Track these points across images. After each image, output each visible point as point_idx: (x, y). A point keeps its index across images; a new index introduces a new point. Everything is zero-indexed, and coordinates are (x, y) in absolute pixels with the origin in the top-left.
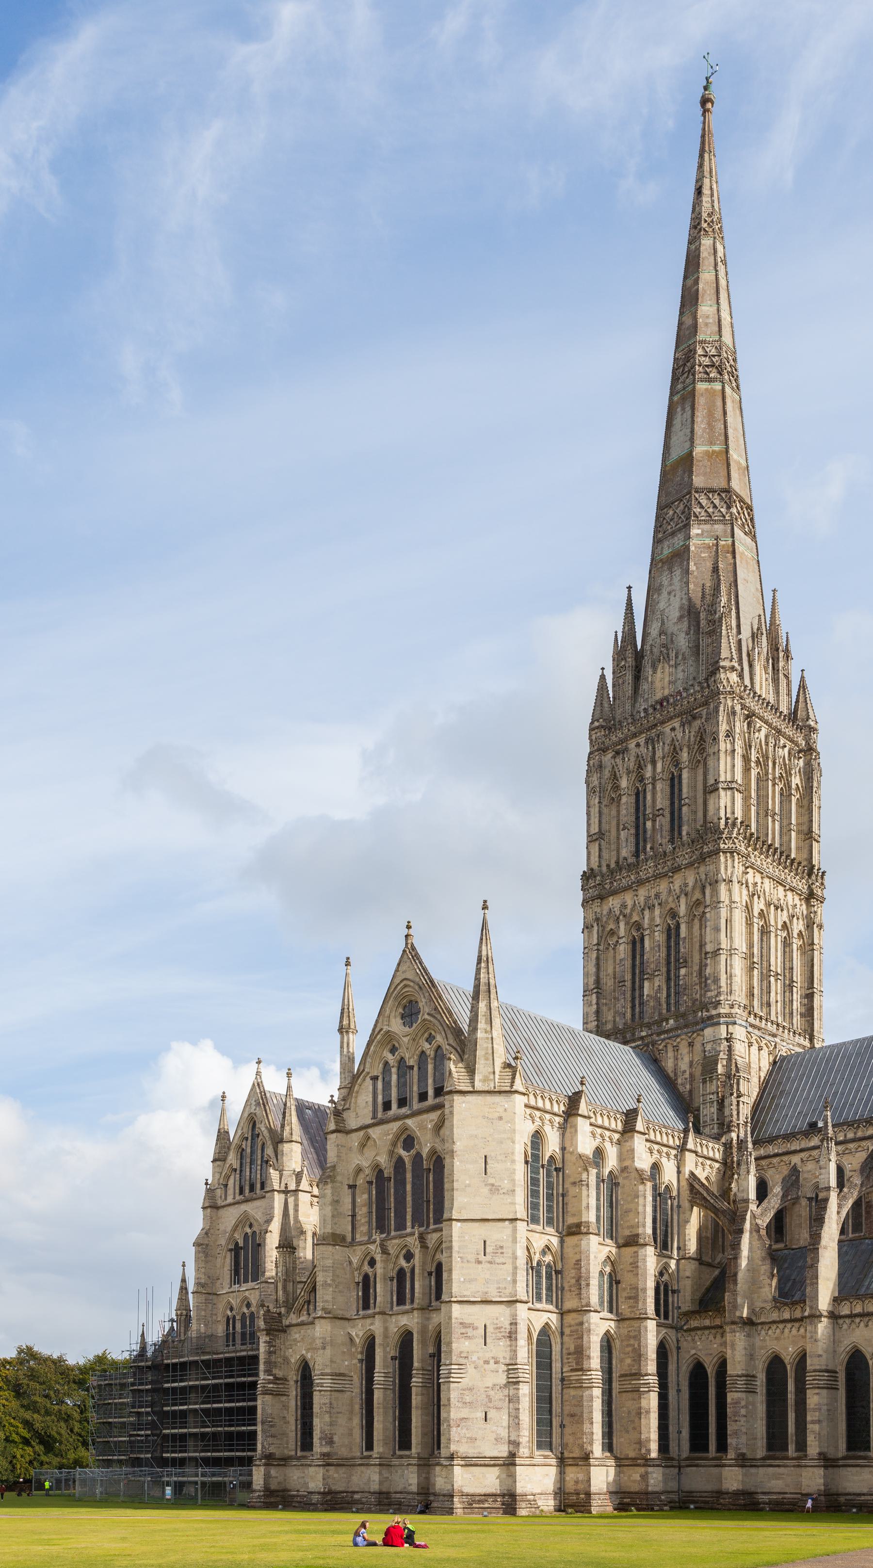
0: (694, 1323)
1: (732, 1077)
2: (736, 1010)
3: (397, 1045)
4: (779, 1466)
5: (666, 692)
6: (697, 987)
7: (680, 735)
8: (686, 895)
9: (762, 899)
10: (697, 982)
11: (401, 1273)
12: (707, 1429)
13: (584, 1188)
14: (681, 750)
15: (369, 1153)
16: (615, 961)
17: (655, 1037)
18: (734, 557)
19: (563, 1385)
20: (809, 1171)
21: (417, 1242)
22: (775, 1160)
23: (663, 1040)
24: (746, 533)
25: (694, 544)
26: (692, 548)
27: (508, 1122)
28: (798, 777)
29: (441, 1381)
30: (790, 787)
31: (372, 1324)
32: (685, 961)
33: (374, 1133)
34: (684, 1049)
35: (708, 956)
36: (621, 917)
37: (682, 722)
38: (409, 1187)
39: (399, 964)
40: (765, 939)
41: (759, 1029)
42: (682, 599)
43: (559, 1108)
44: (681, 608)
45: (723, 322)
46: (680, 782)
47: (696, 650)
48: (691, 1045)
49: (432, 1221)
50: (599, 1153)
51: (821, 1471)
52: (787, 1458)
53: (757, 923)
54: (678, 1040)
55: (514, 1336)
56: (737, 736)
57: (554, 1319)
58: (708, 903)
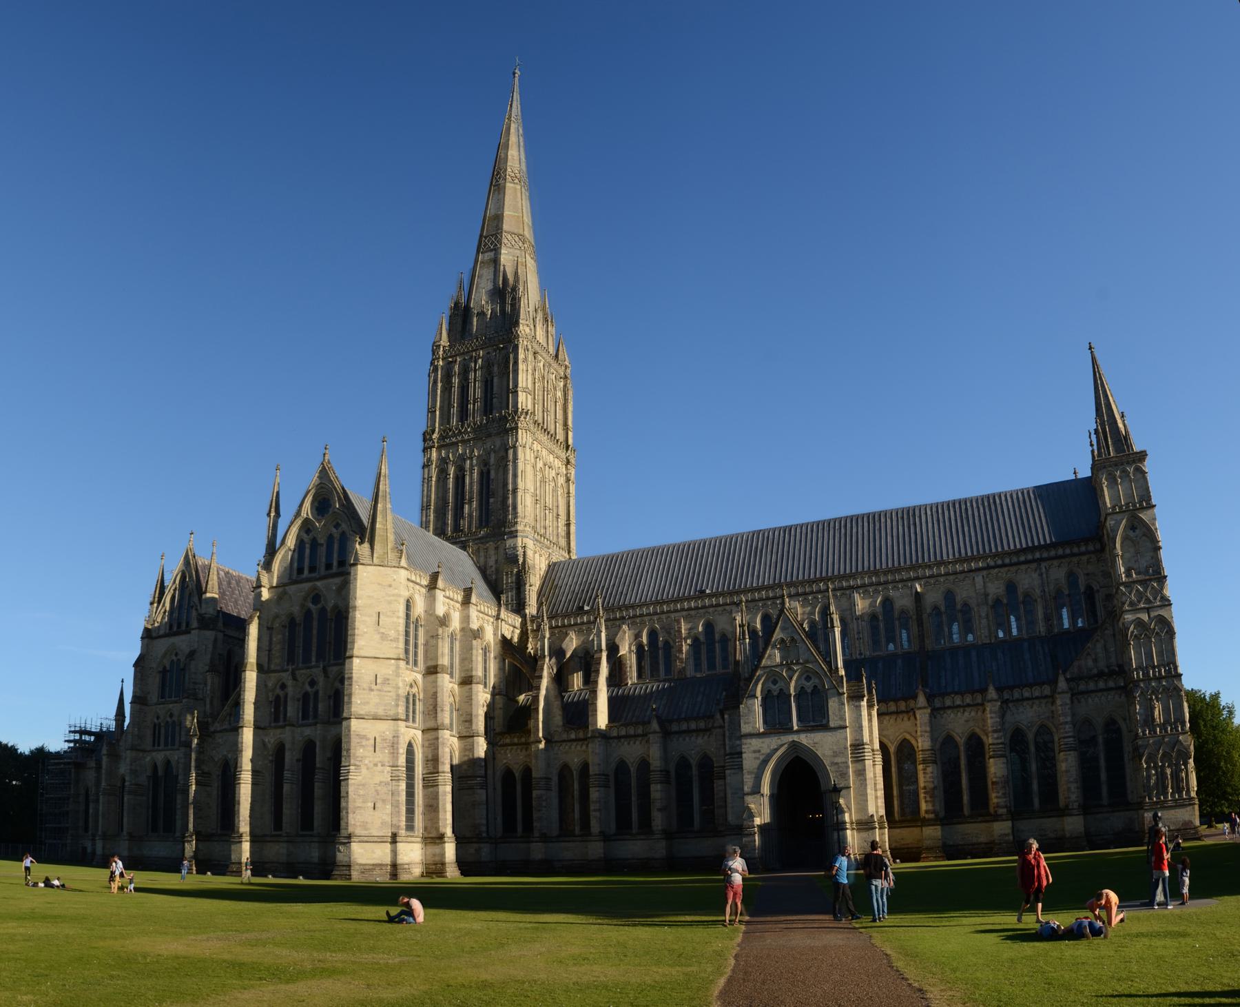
4: (569, 841)
8: (495, 452)
9: (541, 461)
13: (440, 640)
14: (493, 366)
31: (280, 734)
38: (315, 632)
43: (425, 582)
48: (497, 548)
49: (332, 658)
51: (602, 843)
52: (575, 836)
54: (487, 545)
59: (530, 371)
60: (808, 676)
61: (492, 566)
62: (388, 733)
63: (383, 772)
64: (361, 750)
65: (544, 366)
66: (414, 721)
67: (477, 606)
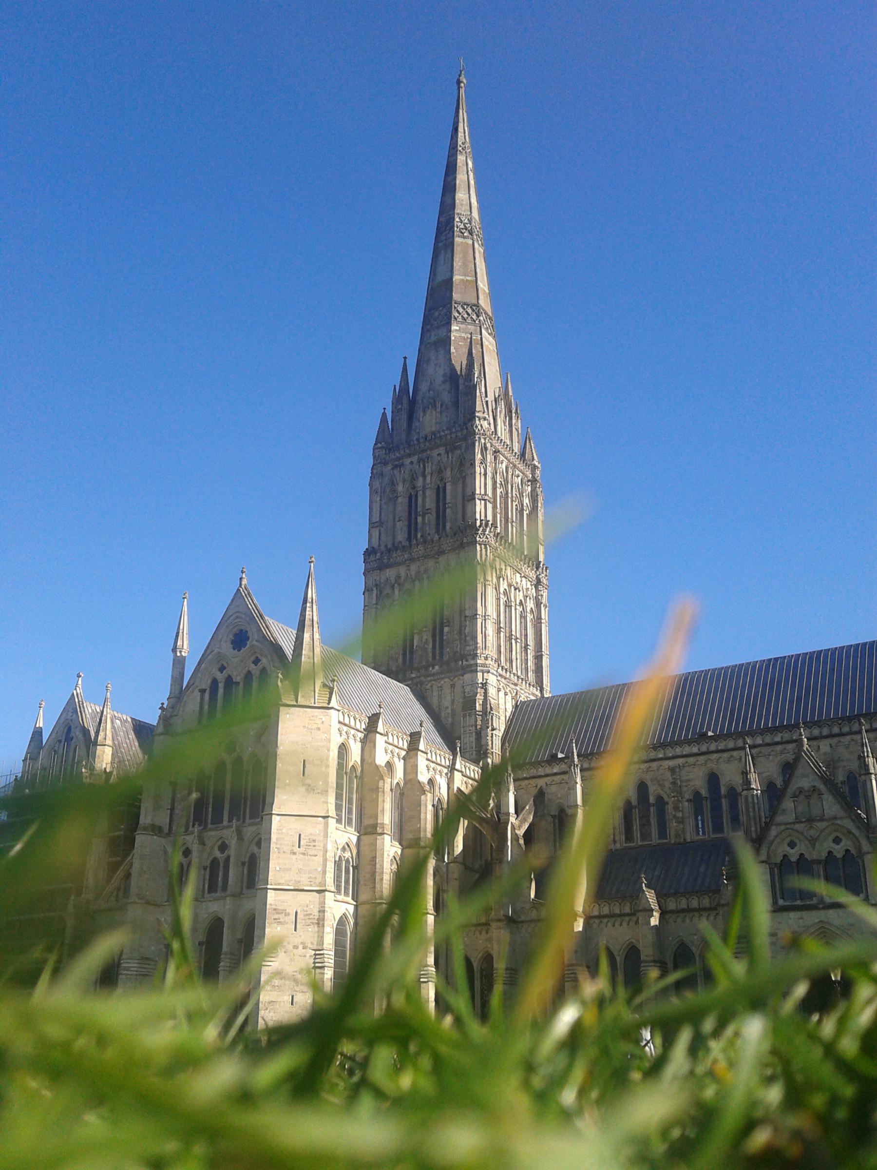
1: (487, 712)
2: (489, 662)
5: (434, 429)
7: (445, 459)
9: (505, 581)
14: (446, 469)
18: (482, 348)
24: (489, 334)
25: (454, 336)
26: (453, 338)
28: (527, 498)
30: (522, 505)
40: (507, 610)
42: (445, 369)
45: (473, 206)
46: (445, 492)
47: (456, 404)
50: (389, 765)
53: (503, 599)
56: (488, 464)
57: (351, 909)
59: (489, 475)
60: (837, 837)
61: (447, 708)
62: (312, 907)
63: (305, 956)
64: (279, 928)
65: (507, 468)
67: (426, 753)
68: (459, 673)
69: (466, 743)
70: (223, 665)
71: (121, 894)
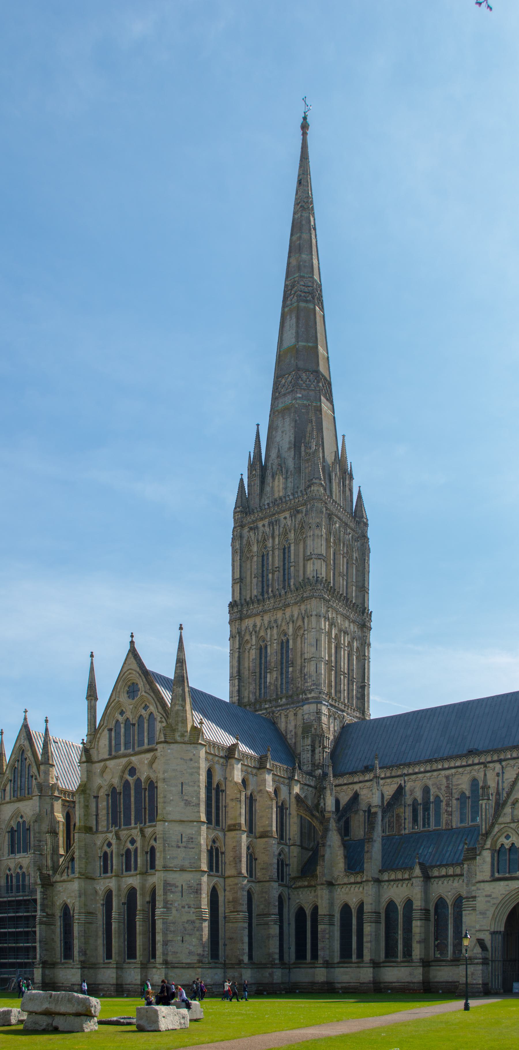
0: (299, 884)
3: (124, 710)
5: (281, 494)
6: (299, 680)
7: (289, 523)
8: (293, 622)
10: (299, 676)
11: (128, 851)
12: (306, 946)
15: (107, 776)
16: (249, 660)
17: (273, 708)
19: (225, 920)
20: (365, 795)
21: (139, 833)
22: (345, 787)
23: (279, 711)
27: (196, 762)
29: (156, 918)
32: (292, 663)
33: (111, 764)
34: (291, 717)
35: (306, 661)
36: (253, 633)
37: (290, 514)
38: (133, 799)
39: (126, 660)
41: (335, 707)
42: (290, 437)
44: (290, 443)
46: (289, 551)
48: (295, 715)
49: (147, 820)
55: (199, 891)
58: (306, 628)
66: (217, 871)
68: (300, 704)
69: (305, 758)
70: (122, 710)
71: (70, 871)
